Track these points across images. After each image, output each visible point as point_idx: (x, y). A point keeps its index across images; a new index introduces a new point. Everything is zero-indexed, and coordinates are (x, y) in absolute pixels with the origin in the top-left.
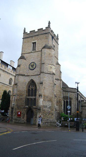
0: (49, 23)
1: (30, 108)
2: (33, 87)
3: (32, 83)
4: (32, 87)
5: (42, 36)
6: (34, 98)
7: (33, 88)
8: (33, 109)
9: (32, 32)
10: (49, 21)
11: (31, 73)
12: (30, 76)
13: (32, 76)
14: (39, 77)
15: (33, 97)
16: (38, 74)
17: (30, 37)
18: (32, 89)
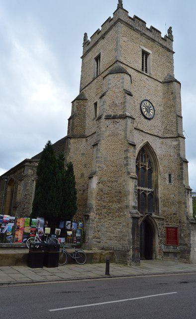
0: (170, 31)
1: (148, 216)
2: (145, 162)
3: (146, 151)
4: (142, 161)
5: (161, 49)
6: (149, 192)
7: (145, 166)
8: (157, 222)
9: (140, 22)
10: (171, 28)
11: (145, 125)
12: (143, 134)
13: (148, 136)
14: (162, 143)
15: (147, 189)
16: (160, 135)
17: (138, 30)
18: (144, 168)
